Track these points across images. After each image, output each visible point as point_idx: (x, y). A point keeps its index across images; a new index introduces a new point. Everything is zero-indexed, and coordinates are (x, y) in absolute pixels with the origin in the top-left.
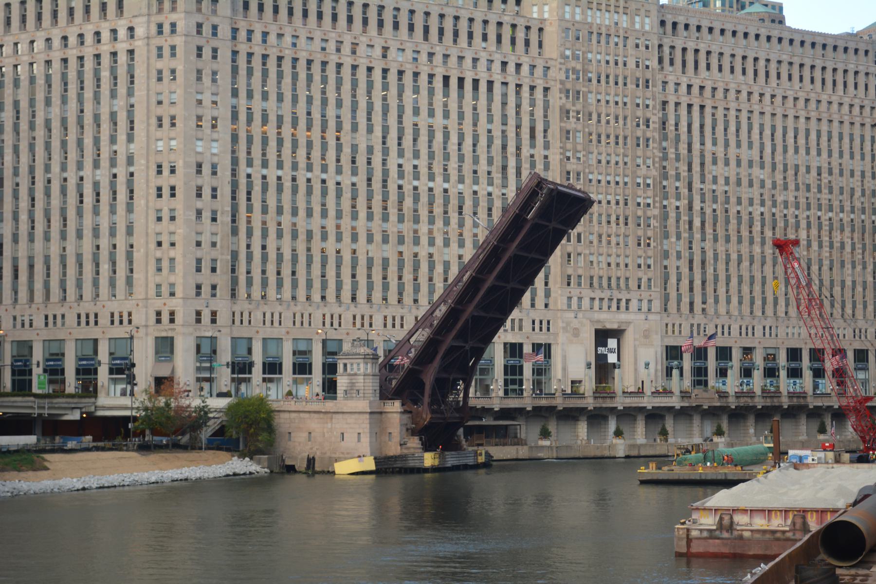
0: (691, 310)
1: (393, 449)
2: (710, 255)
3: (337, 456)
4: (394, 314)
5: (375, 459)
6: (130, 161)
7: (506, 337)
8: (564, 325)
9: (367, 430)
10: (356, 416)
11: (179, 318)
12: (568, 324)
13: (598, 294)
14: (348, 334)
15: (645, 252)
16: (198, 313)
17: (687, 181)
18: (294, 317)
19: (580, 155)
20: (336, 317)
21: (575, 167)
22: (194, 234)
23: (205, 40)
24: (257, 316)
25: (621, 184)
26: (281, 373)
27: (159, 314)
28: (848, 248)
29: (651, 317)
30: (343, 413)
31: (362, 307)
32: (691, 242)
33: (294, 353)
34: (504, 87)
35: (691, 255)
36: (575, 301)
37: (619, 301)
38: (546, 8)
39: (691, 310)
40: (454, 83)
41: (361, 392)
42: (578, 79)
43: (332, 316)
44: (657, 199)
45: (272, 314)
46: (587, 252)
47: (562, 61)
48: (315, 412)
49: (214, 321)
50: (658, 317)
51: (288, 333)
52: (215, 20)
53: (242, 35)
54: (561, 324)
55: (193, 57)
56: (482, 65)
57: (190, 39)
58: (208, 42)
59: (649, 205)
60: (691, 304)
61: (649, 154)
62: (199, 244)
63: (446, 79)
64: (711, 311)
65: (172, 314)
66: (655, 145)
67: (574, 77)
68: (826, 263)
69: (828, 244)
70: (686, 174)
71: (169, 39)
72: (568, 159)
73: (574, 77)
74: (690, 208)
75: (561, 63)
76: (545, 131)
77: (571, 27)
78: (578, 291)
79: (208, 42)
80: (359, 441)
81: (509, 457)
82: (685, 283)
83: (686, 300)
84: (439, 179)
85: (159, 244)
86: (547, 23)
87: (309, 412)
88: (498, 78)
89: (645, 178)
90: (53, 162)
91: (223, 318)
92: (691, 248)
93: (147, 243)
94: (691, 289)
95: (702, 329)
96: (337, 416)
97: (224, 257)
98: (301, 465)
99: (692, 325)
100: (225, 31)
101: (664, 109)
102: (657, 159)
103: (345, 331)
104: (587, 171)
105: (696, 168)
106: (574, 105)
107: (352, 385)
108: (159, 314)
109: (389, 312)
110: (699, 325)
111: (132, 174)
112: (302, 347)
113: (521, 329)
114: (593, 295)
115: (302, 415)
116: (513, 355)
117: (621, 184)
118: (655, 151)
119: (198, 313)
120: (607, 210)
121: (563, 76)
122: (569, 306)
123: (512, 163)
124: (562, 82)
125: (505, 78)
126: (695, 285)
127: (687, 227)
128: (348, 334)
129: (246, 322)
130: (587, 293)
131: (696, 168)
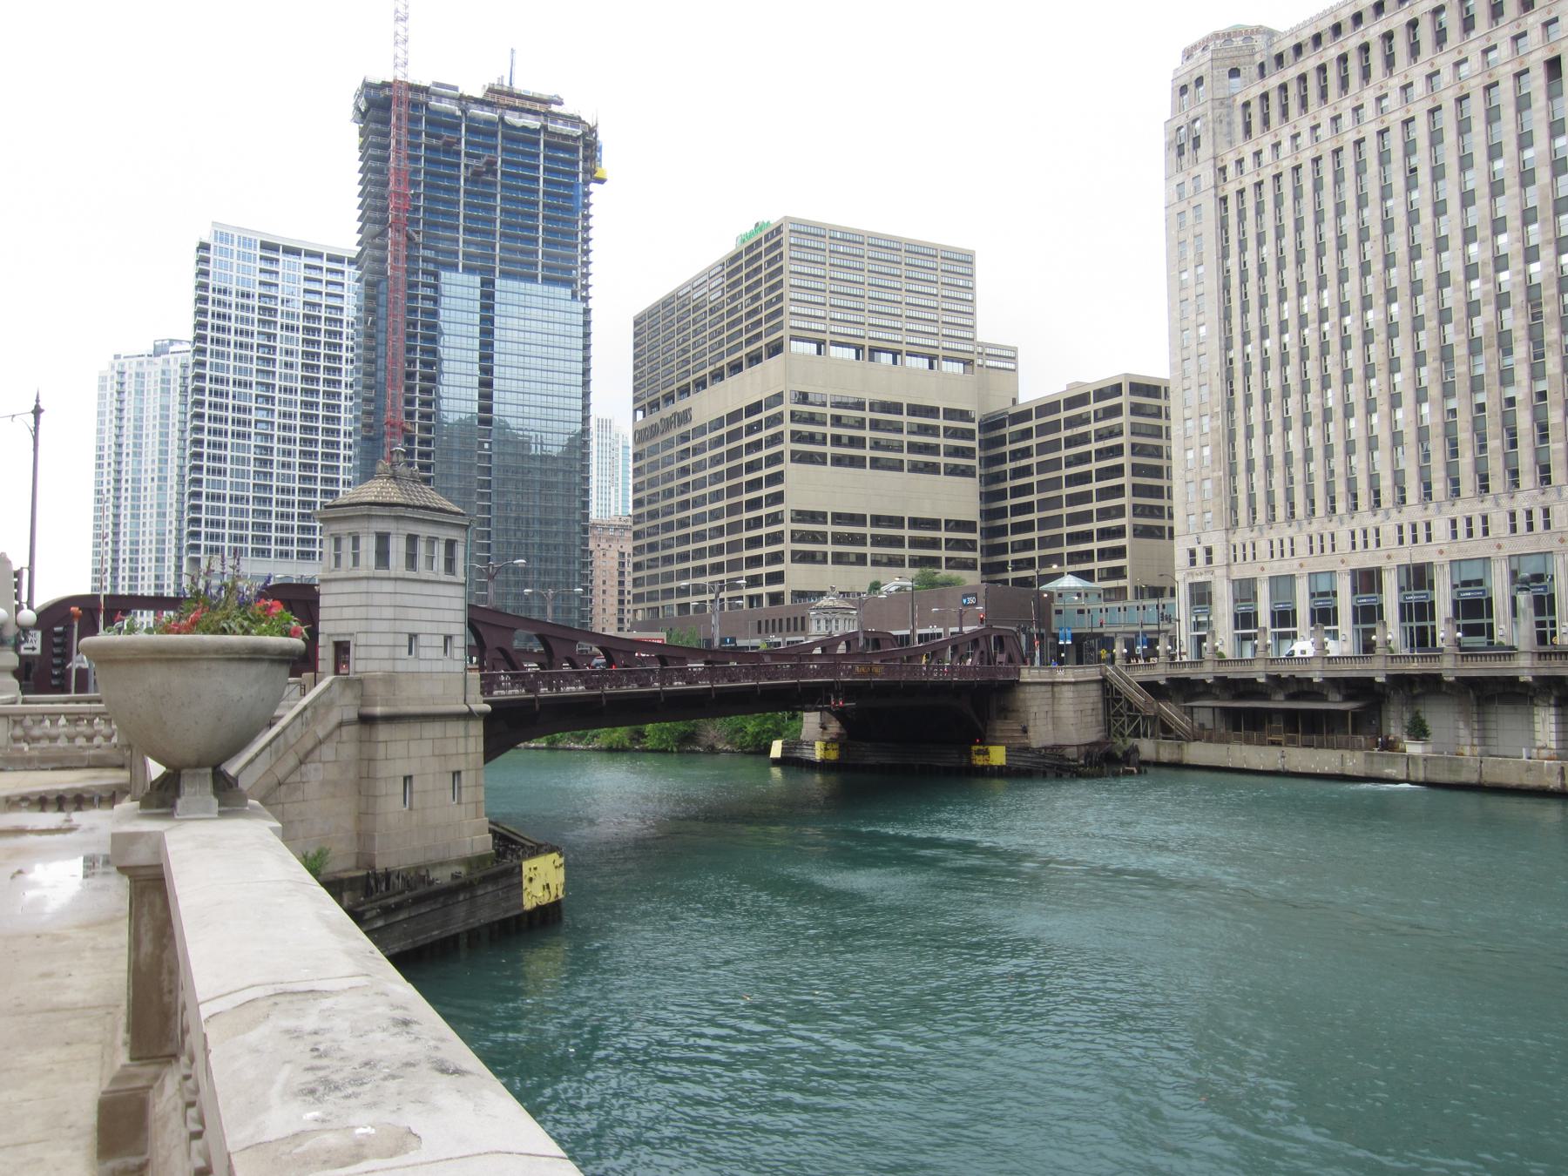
4: (1468, 514)
14: (1389, 557)
27: (1192, 553)
33: (1312, 595)
43: (1365, 532)
51: (1301, 565)
65: (1209, 551)
103: (1386, 553)
108: (1192, 553)
112: (1323, 587)
128: (1389, 557)
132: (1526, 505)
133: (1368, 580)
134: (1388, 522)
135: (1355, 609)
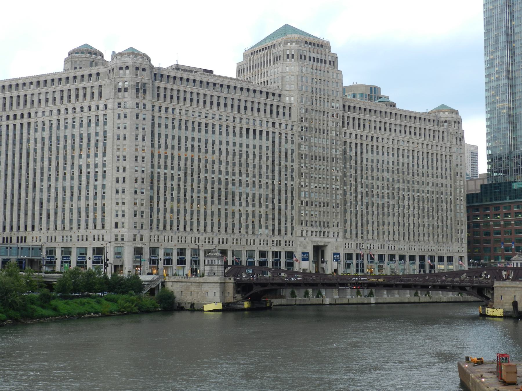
0: (357, 237)
1: (230, 299)
2: (365, 211)
3: (205, 302)
5: (222, 304)
6: (104, 165)
7: (273, 248)
8: (300, 243)
9: (219, 291)
10: (214, 284)
11: (126, 239)
12: (301, 243)
13: (315, 229)
15: (336, 210)
16: (135, 236)
17: (355, 178)
18: (178, 238)
19: (307, 165)
20: (197, 238)
21: (305, 171)
22: (133, 199)
23: (140, 111)
24: (161, 237)
25: (325, 179)
26: (172, 264)
28: (426, 210)
29: (338, 240)
30: (207, 283)
31: (209, 234)
32: (356, 206)
34: (274, 134)
35: (357, 211)
36: (304, 232)
37: (324, 232)
38: (292, 98)
39: (357, 237)
40: (251, 132)
41: (216, 273)
42: (307, 131)
43: (195, 238)
44: (342, 186)
45: (168, 237)
46: (310, 210)
47: (300, 122)
48: (194, 282)
49: (142, 240)
50: (342, 240)
51: (175, 245)
52: (145, 102)
53: (157, 108)
55: (134, 118)
56: (264, 124)
57: (133, 110)
58: (141, 111)
59: (338, 189)
60: (357, 234)
61: (338, 165)
63: (248, 130)
64: (365, 237)
66: (341, 161)
67: (305, 130)
68: (416, 216)
69: (417, 207)
70: (354, 175)
71: (123, 110)
72: (302, 167)
73: (305, 130)
74: (356, 190)
75: (299, 124)
76: (292, 154)
77: (304, 107)
78: (306, 228)
79: (141, 111)
80: (215, 296)
81: (278, 304)
82: (354, 224)
83: (354, 232)
84: (244, 176)
85: (117, 204)
86: (293, 105)
87: (191, 282)
88: (271, 130)
89: (336, 176)
90: (67, 165)
91: (146, 239)
92: (356, 209)
93: (112, 203)
94: (356, 227)
95: (361, 245)
96: (204, 284)
97: (147, 210)
98: (188, 307)
99: (357, 244)
100: (149, 107)
101: (345, 145)
102: (342, 168)
104: (310, 173)
105: (359, 172)
106: (305, 142)
107: (212, 270)
109: (221, 236)
110: (360, 244)
111: (105, 171)
113: (280, 244)
114: (313, 230)
115: (188, 284)
116: (277, 257)
117: (325, 179)
119: (135, 236)
120: (319, 190)
121: (300, 129)
122: (302, 235)
123: (277, 168)
124: (300, 132)
125: (274, 130)
126: (358, 226)
127: (355, 199)
129: (156, 240)
130: (310, 229)
131: (359, 172)
132: (237, 238)
133: (182, 252)
134: (203, 236)
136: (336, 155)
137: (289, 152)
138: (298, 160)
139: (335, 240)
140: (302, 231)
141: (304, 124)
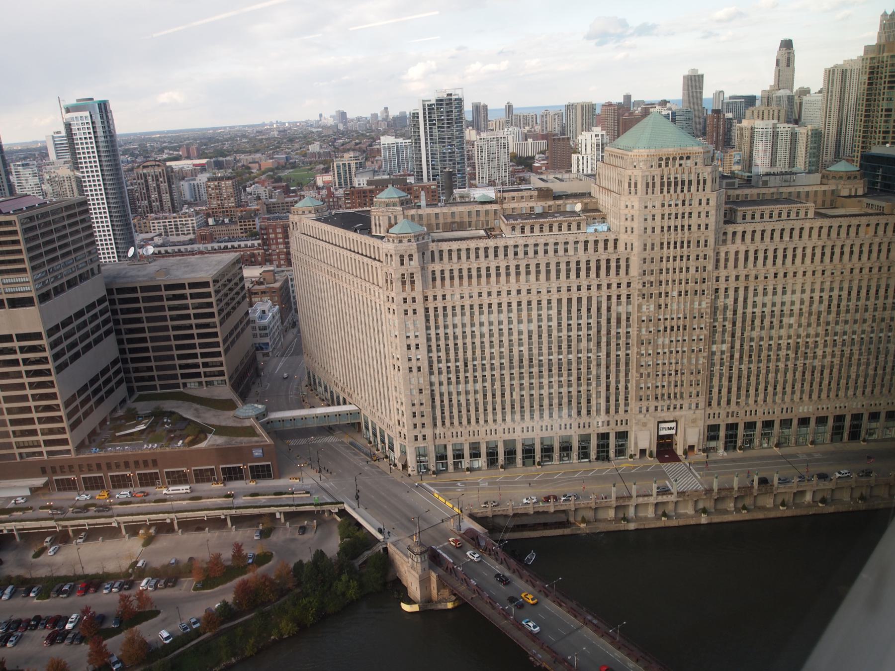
16: (416, 436)
29: (697, 412)
52: (413, 294)
54: (634, 421)
55: (403, 315)
62: (413, 405)
64: (742, 403)
91: (429, 437)
100: (420, 298)
118: (707, 320)
121: (641, 286)
122: (640, 412)
124: (639, 290)
130: (652, 404)
135: (487, 453)
136: (699, 310)
137: (624, 317)
138: (636, 325)
139: (692, 412)
140: (641, 408)
141: (648, 278)
